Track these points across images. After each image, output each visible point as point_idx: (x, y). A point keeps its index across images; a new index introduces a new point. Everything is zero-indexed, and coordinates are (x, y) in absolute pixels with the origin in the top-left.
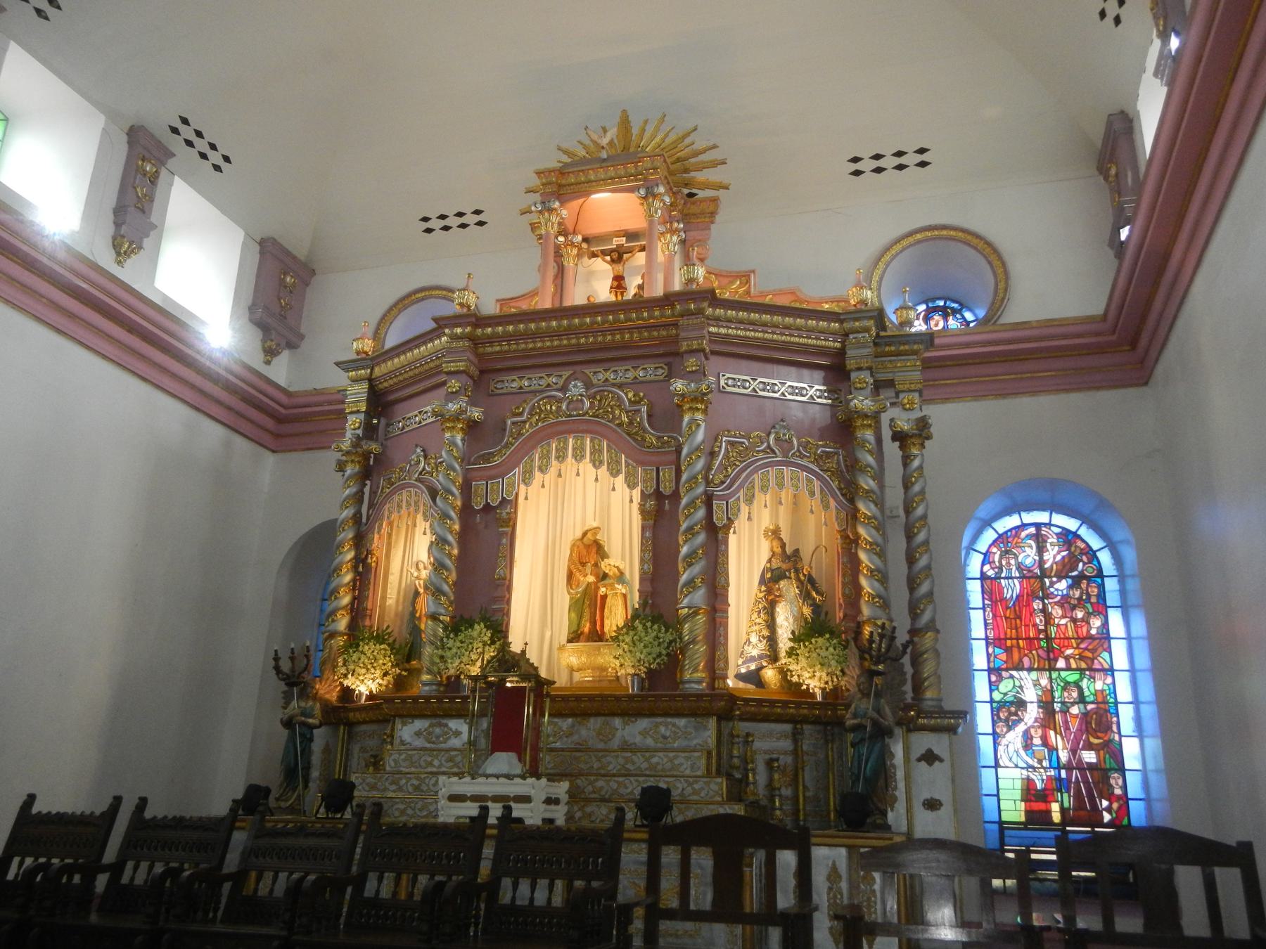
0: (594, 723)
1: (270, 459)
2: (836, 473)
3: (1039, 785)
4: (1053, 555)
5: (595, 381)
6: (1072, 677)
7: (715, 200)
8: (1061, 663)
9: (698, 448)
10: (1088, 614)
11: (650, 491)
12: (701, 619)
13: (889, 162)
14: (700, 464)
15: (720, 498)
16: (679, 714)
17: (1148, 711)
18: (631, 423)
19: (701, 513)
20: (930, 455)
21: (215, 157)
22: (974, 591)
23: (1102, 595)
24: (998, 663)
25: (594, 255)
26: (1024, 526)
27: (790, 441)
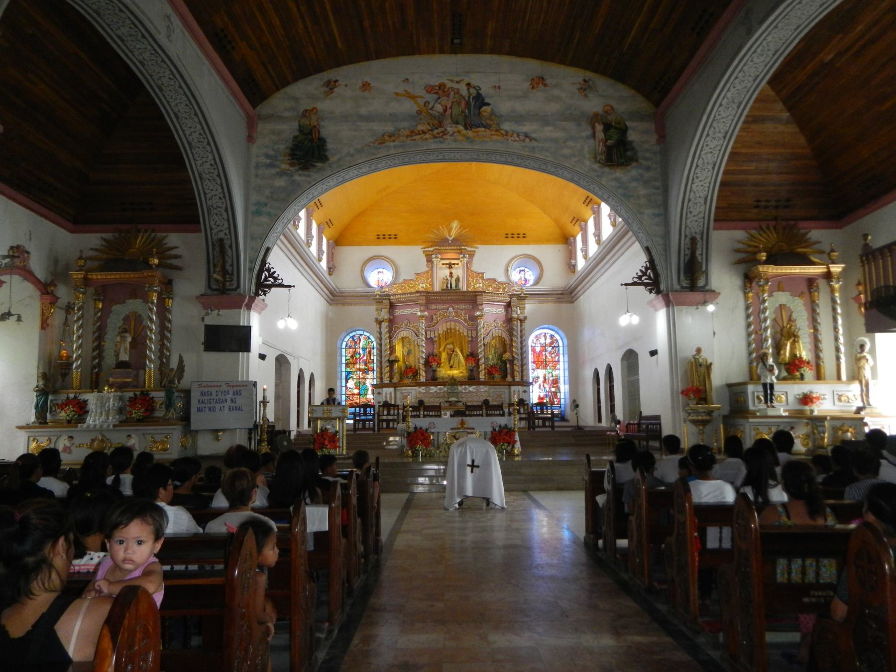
1: (330, 307)
2: (508, 330)
3: (542, 396)
4: (548, 341)
6: (550, 371)
7: (475, 251)
8: (548, 368)
10: (555, 356)
13: (516, 236)
17: (567, 379)
20: (527, 324)
21: (331, 225)
22: (530, 349)
23: (559, 351)
24: (534, 368)
25: (443, 264)
26: (541, 334)
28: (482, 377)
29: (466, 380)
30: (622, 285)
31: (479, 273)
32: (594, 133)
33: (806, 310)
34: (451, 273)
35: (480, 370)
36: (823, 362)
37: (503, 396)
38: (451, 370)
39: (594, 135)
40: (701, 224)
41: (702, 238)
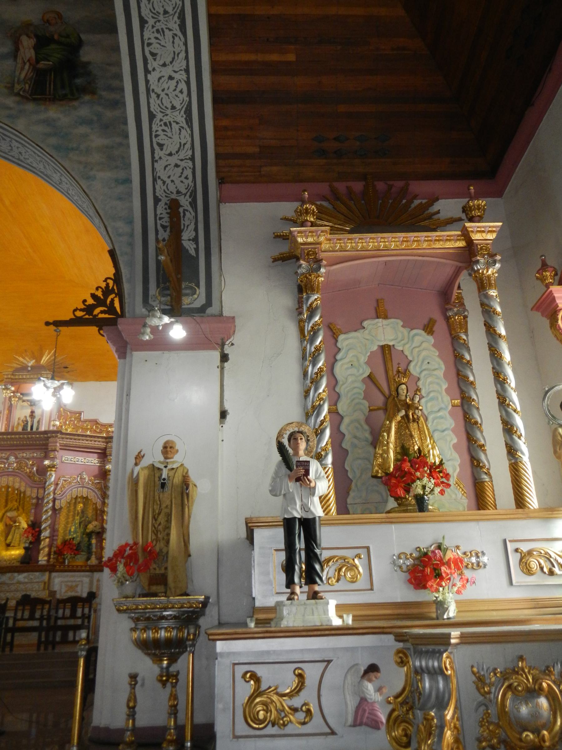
0: (9, 575)
2: (100, 489)
5: (19, 456)
9: (52, 484)
11: (35, 496)
12: (47, 540)
14: (52, 489)
15: (58, 499)
16: (37, 571)
18: (30, 472)
19: (51, 505)
25: (24, 401)
27: (85, 479)
28: (42, 559)
29: (18, 564)
30: (47, 324)
31: (75, 413)
32: (17, 50)
33: (440, 356)
34: (32, 412)
35: (41, 546)
36: (488, 474)
37: (79, 589)
38: (7, 550)
39: (15, 54)
40: (189, 172)
41: (193, 204)
